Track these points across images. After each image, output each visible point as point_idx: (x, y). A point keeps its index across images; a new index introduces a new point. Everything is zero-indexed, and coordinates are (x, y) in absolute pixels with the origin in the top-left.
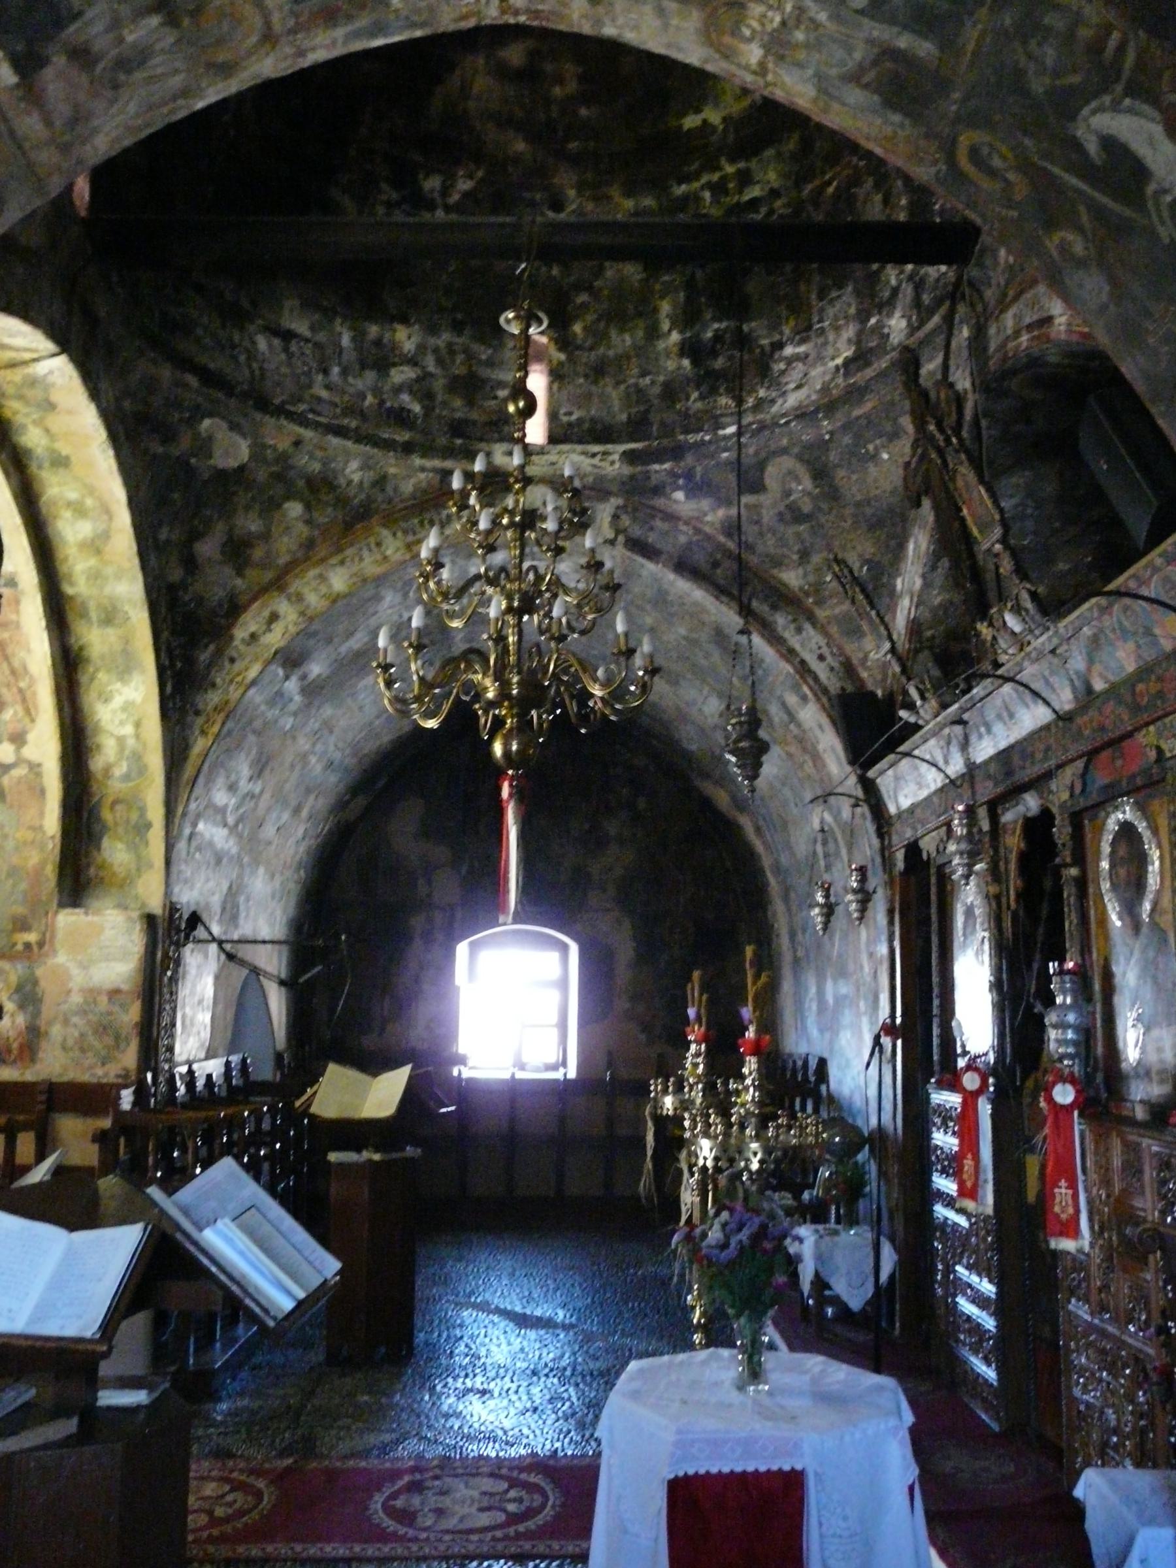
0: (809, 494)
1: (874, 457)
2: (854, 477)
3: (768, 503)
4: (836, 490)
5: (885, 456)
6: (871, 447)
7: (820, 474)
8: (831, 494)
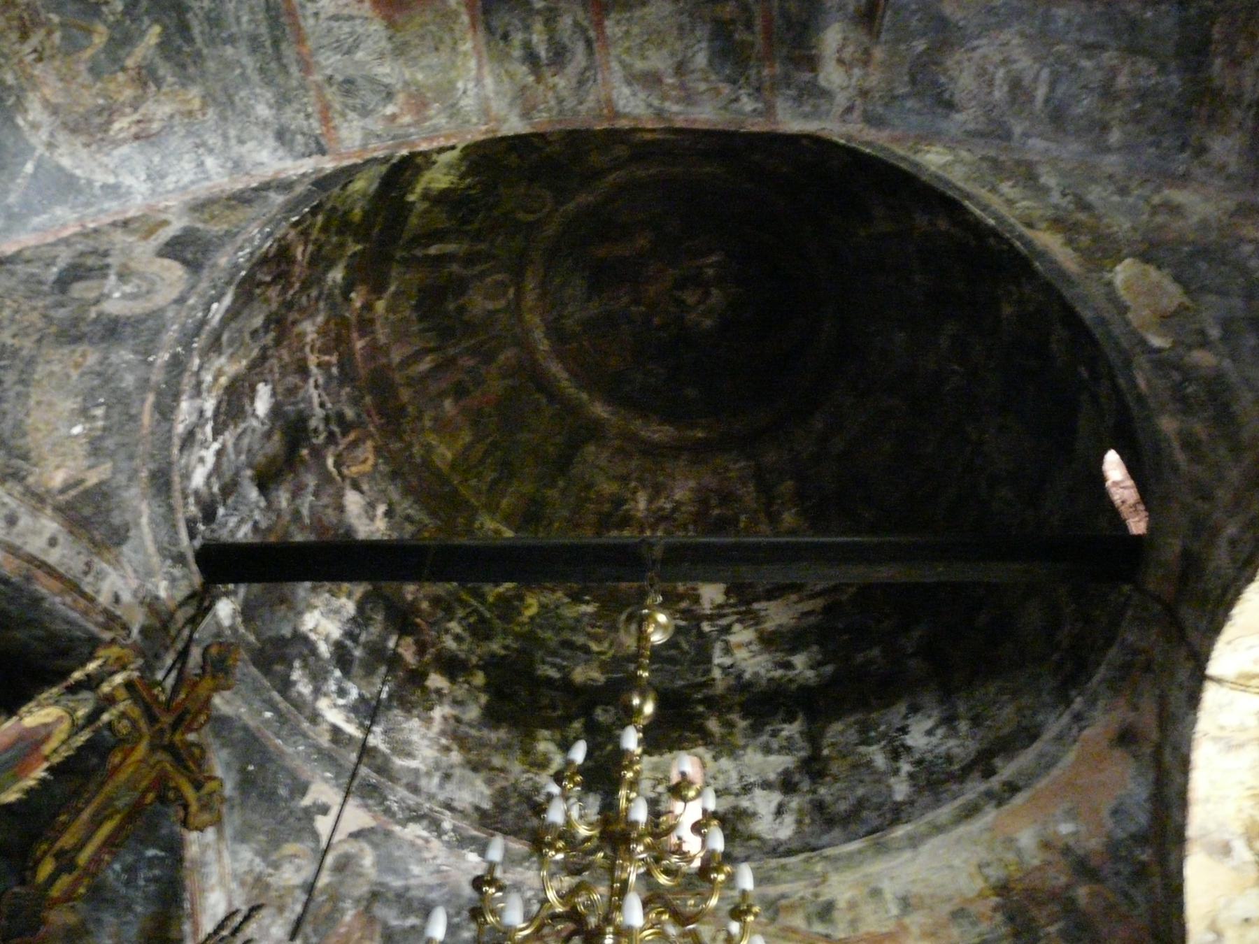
0: (97, 301)
1: (84, 413)
2: (75, 374)
4: (78, 339)
5: (77, 430)
6: (99, 412)
7: (112, 330)
8: (71, 334)
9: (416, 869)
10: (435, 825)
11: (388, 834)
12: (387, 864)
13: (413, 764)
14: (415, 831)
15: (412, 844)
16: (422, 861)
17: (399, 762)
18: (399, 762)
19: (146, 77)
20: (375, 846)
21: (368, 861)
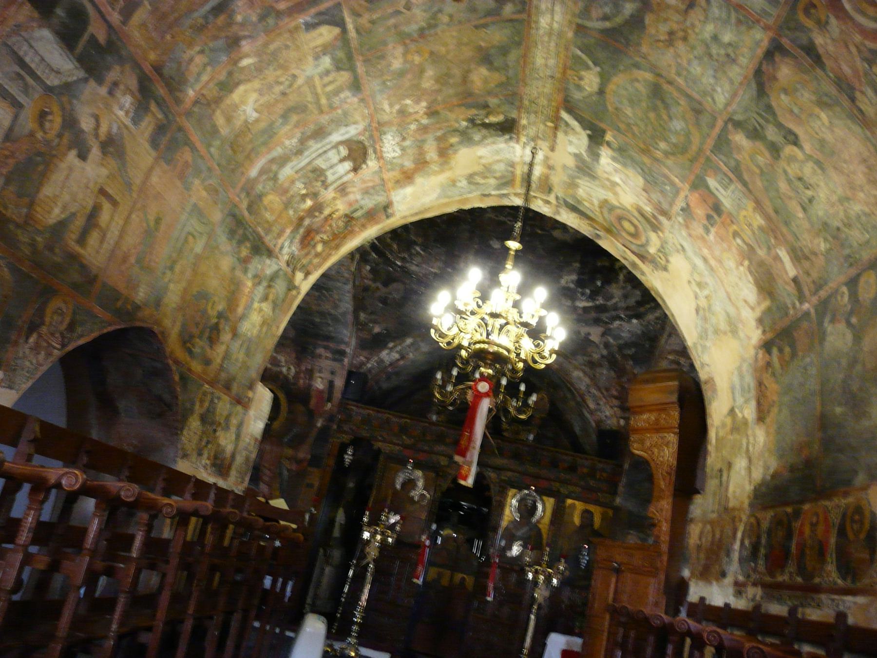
3: (383, 291)
9: (623, 335)
10: (621, 319)
11: (610, 329)
12: (616, 338)
13: (614, 301)
14: (617, 323)
15: (618, 328)
16: (623, 331)
17: (609, 303)
18: (609, 303)
19: (331, 296)
20: (609, 335)
21: (611, 341)
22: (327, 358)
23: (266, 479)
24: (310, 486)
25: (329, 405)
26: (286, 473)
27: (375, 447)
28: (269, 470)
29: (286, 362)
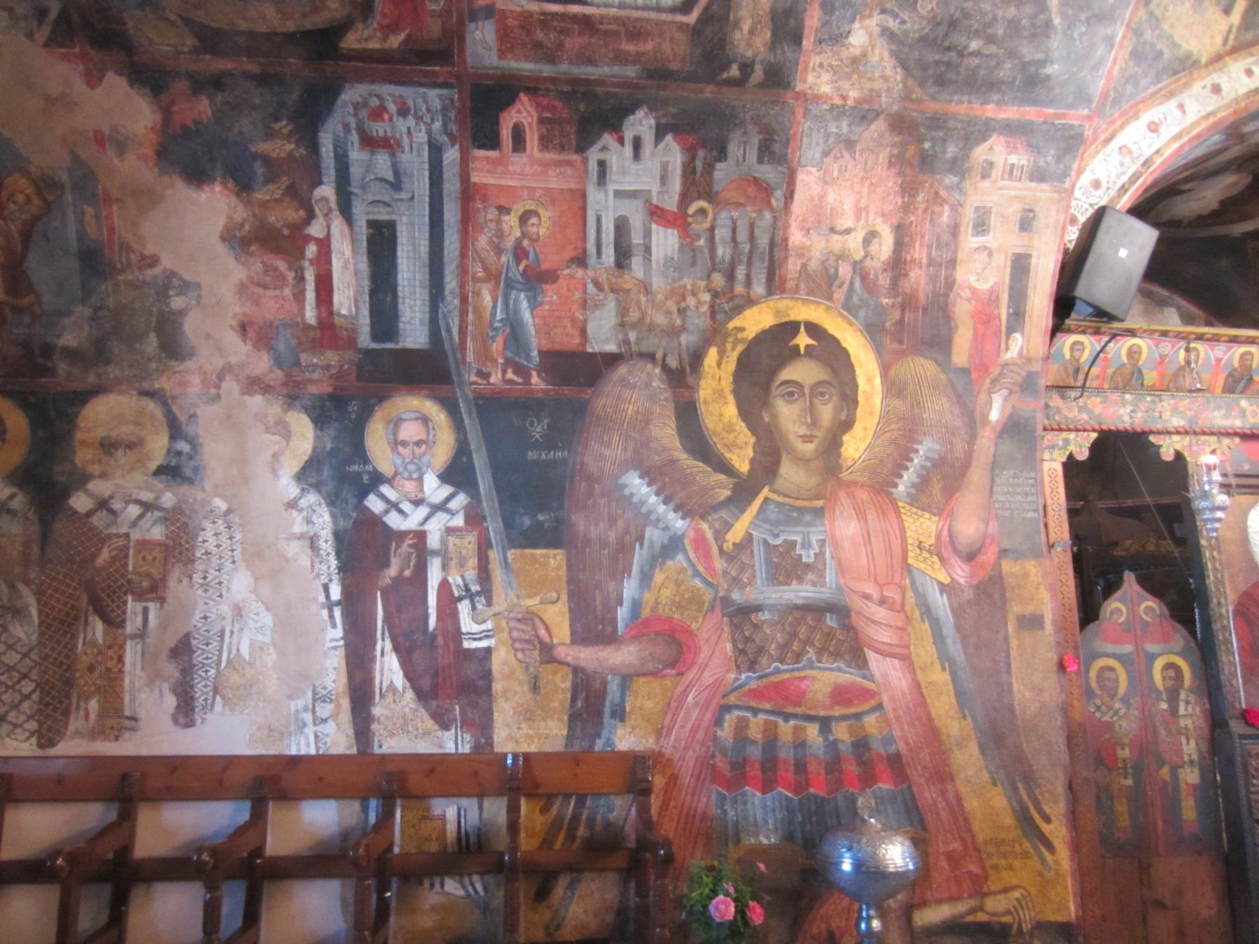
22: (1010, 171)
23: (884, 636)
24: (1032, 622)
25: (1017, 341)
26: (941, 603)
27: (1167, 455)
28: (882, 602)
29: (859, 213)
